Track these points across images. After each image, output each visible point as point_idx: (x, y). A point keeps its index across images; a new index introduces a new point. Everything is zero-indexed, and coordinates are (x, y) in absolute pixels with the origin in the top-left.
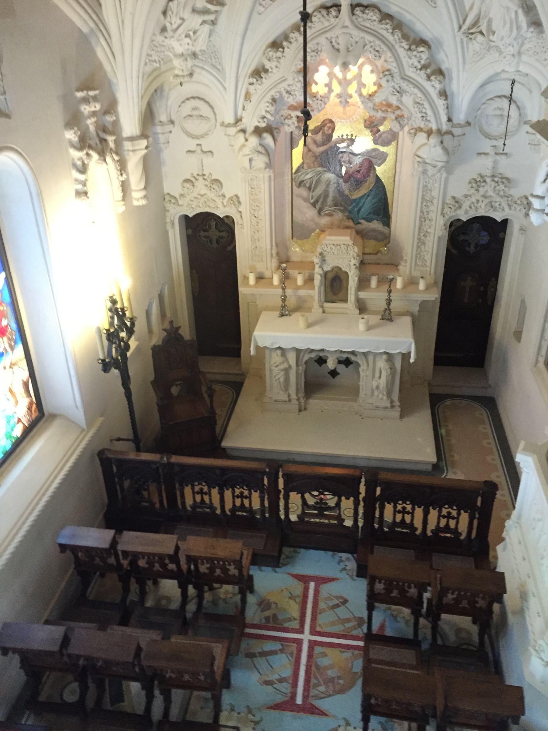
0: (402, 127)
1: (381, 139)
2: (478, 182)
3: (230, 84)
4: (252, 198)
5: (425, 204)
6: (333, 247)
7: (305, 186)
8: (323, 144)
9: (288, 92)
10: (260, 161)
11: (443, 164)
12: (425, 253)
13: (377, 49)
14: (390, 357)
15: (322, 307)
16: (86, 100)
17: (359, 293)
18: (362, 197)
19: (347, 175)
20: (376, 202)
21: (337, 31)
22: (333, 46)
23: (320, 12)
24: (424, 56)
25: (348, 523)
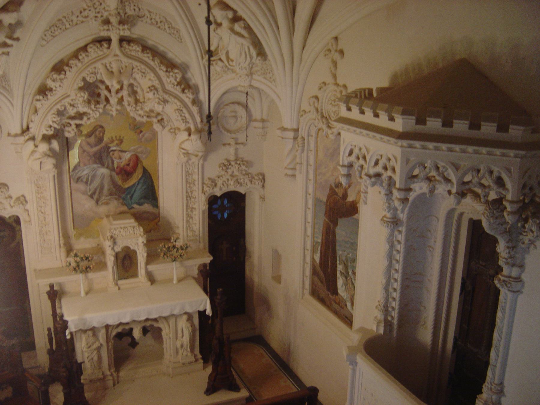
0: (164, 127)
2: (226, 165)
3: (17, 102)
4: (39, 196)
5: (188, 185)
6: (122, 230)
7: (82, 181)
8: (96, 145)
9: (71, 105)
10: (49, 163)
11: (202, 154)
12: (193, 225)
13: (143, 71)
14: (190, 316)
15: (117, 284)
18: (134, 185)
19: (119, 169)
20: (145, 189)
21: (111, 59)
22: (108, 70)
23: (95, 45)
24: (179, 76)
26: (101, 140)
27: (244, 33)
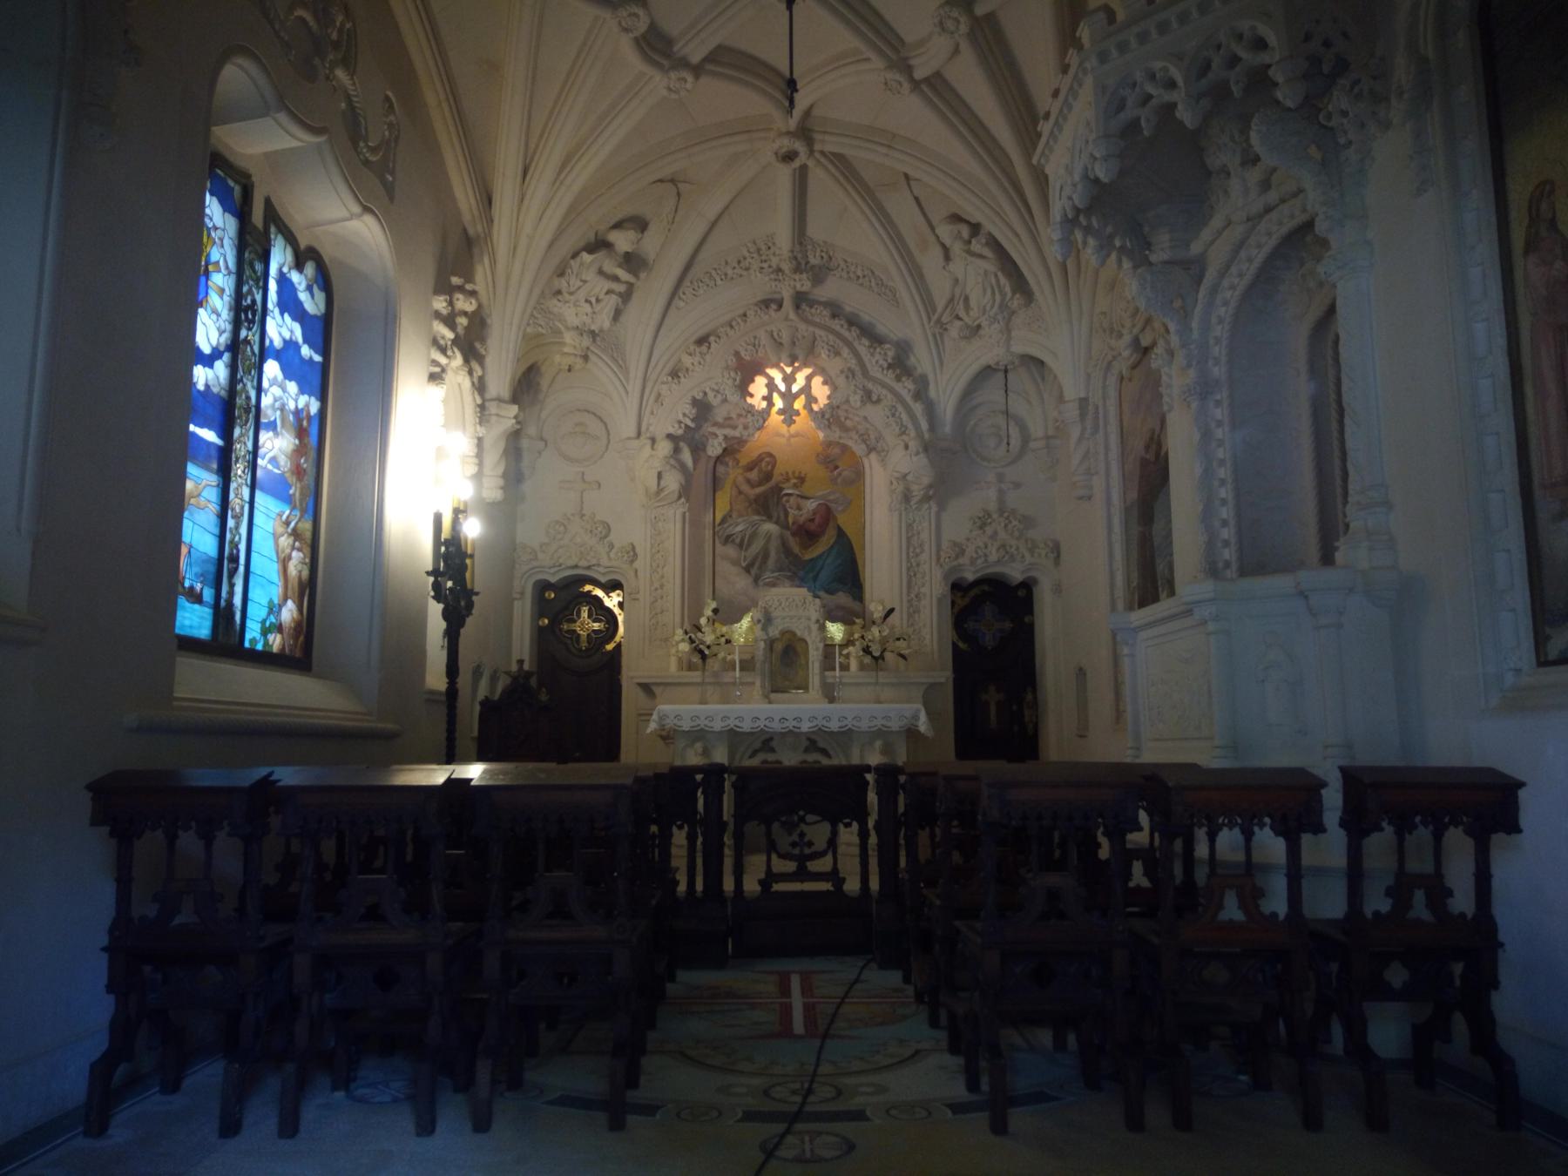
2: (982, 522)
3: (635, 386)
8: (760, 484)
16: (461, 289)
18: (820, 556)
24: (891, 354)
25: (852, 886)
26: (768, 476)
27: (987, 252)
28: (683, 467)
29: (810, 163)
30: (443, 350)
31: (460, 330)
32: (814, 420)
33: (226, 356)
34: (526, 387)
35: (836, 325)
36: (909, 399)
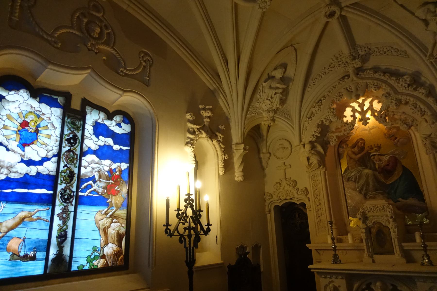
1: (399, 143)
3: (296, 126)
8: (359, 153)
9: (325, 119)
13: (376, 84)
15: (372, 257)
16: (204, 109)
17: (403, 244)
18: (395, 181)
22: (349, 91)
24: (408, 80)
26: (362, 149)
28: (319, 153)
29: (343, 13)
30: (193, 133)
31: (206, 123)
32: (377, 120)
33: (55, 159)
34: (255, 136)
35: (377, 76)
36: (423, 97)
